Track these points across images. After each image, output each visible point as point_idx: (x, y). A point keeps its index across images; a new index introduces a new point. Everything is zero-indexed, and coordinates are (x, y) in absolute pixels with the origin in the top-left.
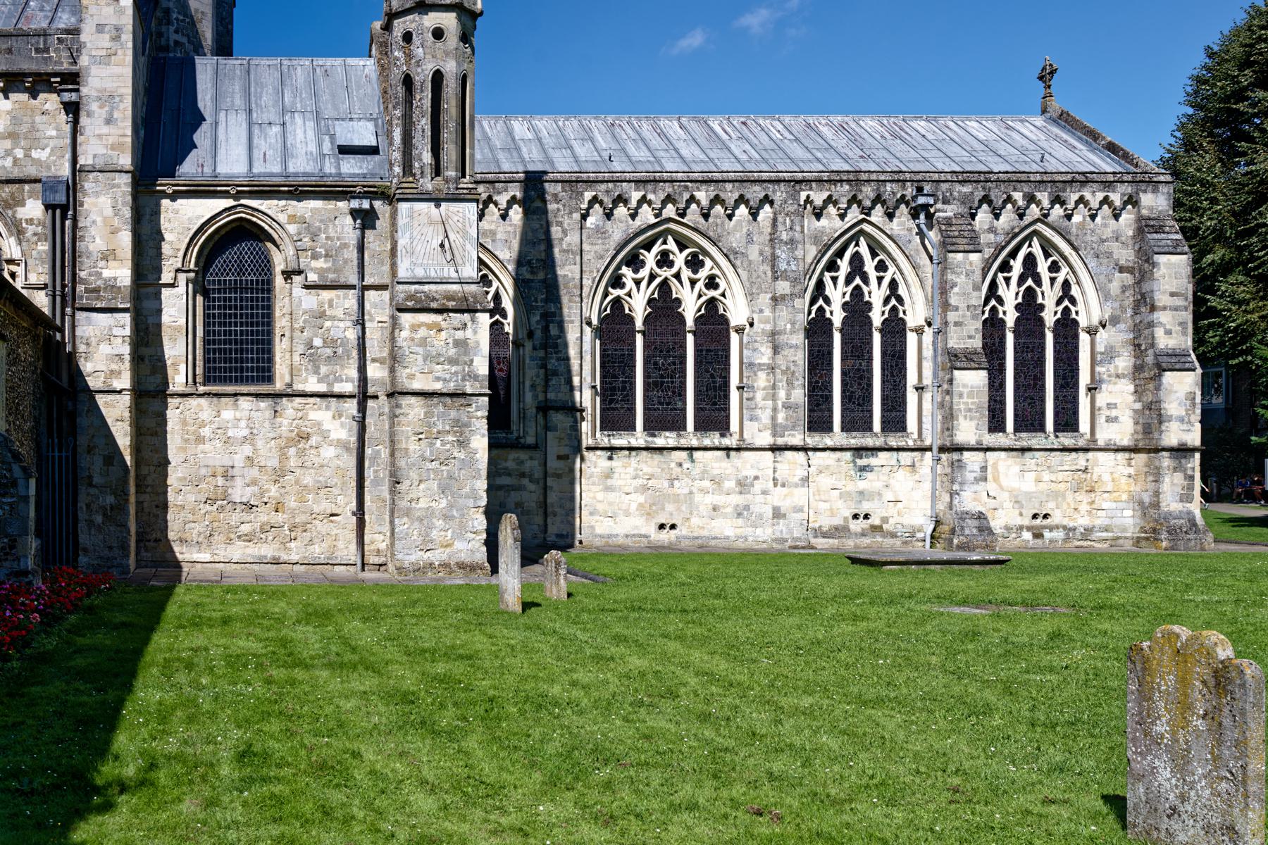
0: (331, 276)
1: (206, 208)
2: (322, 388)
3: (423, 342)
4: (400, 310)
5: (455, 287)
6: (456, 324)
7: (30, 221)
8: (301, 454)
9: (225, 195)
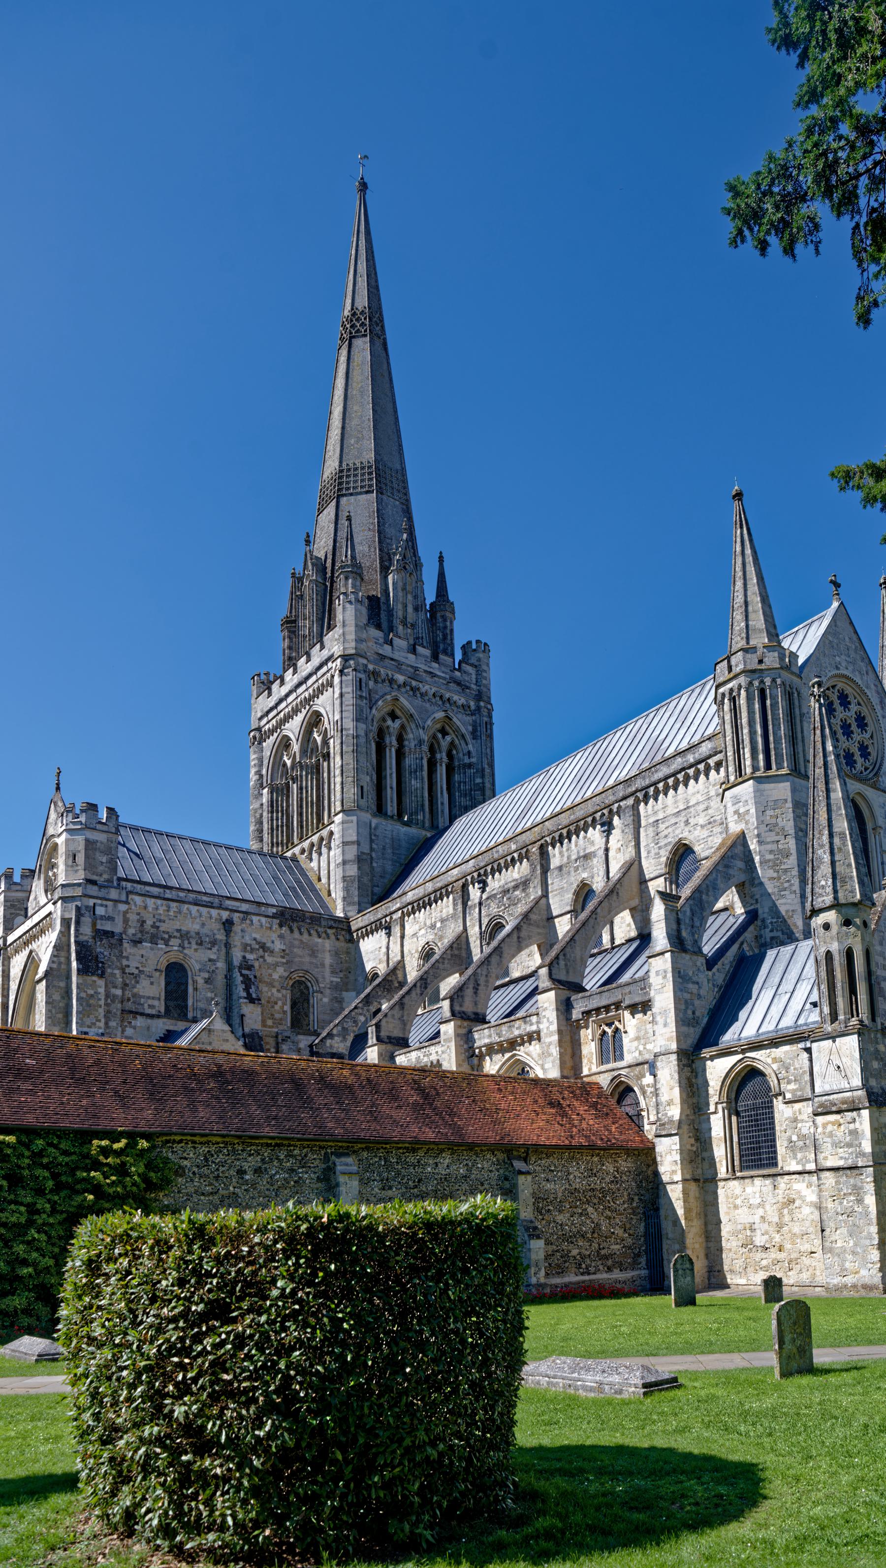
0: (799, 1093)
1: (727, 1062)
2: (799, 1168)
3: (831, 1135)
4: (815, 1115)
5: (849, 1094)
6: (849, 1119)
7: (648, 1086)
8: (791, 1213)
9: (735, 1053)
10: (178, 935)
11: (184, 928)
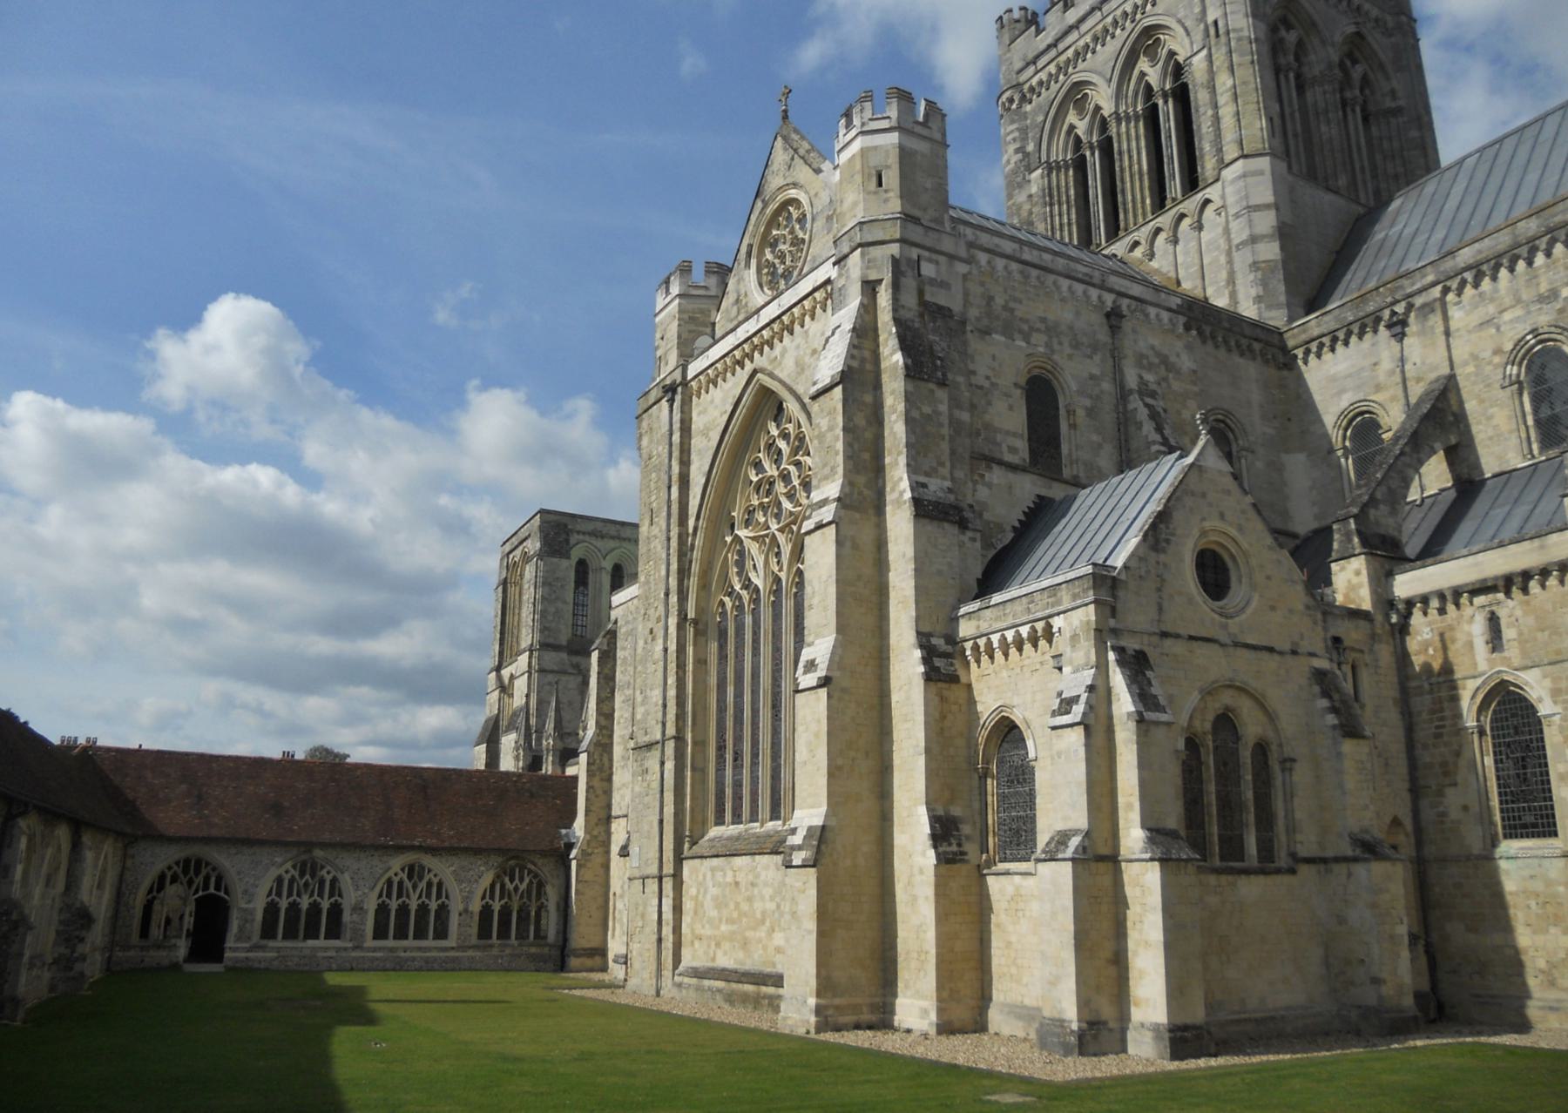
10: (1042, 326)
11: (1051, 317)
